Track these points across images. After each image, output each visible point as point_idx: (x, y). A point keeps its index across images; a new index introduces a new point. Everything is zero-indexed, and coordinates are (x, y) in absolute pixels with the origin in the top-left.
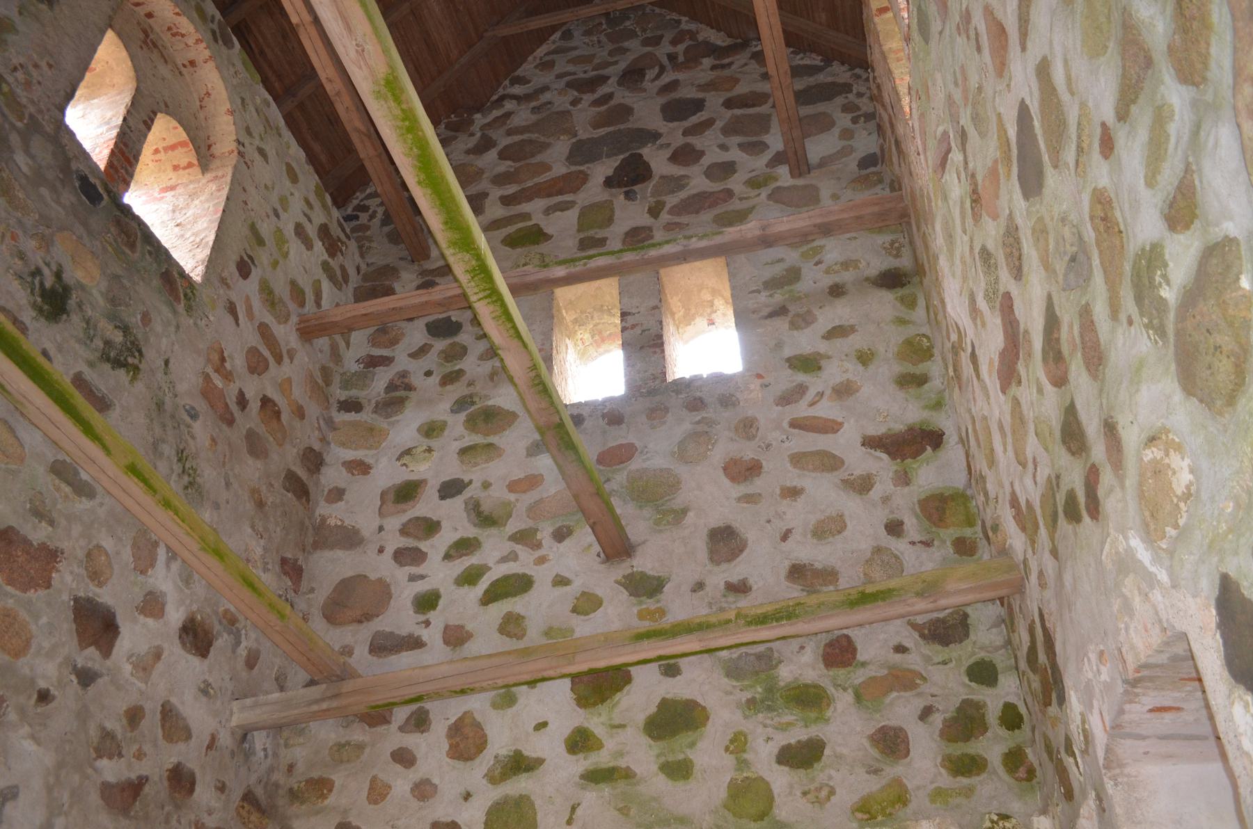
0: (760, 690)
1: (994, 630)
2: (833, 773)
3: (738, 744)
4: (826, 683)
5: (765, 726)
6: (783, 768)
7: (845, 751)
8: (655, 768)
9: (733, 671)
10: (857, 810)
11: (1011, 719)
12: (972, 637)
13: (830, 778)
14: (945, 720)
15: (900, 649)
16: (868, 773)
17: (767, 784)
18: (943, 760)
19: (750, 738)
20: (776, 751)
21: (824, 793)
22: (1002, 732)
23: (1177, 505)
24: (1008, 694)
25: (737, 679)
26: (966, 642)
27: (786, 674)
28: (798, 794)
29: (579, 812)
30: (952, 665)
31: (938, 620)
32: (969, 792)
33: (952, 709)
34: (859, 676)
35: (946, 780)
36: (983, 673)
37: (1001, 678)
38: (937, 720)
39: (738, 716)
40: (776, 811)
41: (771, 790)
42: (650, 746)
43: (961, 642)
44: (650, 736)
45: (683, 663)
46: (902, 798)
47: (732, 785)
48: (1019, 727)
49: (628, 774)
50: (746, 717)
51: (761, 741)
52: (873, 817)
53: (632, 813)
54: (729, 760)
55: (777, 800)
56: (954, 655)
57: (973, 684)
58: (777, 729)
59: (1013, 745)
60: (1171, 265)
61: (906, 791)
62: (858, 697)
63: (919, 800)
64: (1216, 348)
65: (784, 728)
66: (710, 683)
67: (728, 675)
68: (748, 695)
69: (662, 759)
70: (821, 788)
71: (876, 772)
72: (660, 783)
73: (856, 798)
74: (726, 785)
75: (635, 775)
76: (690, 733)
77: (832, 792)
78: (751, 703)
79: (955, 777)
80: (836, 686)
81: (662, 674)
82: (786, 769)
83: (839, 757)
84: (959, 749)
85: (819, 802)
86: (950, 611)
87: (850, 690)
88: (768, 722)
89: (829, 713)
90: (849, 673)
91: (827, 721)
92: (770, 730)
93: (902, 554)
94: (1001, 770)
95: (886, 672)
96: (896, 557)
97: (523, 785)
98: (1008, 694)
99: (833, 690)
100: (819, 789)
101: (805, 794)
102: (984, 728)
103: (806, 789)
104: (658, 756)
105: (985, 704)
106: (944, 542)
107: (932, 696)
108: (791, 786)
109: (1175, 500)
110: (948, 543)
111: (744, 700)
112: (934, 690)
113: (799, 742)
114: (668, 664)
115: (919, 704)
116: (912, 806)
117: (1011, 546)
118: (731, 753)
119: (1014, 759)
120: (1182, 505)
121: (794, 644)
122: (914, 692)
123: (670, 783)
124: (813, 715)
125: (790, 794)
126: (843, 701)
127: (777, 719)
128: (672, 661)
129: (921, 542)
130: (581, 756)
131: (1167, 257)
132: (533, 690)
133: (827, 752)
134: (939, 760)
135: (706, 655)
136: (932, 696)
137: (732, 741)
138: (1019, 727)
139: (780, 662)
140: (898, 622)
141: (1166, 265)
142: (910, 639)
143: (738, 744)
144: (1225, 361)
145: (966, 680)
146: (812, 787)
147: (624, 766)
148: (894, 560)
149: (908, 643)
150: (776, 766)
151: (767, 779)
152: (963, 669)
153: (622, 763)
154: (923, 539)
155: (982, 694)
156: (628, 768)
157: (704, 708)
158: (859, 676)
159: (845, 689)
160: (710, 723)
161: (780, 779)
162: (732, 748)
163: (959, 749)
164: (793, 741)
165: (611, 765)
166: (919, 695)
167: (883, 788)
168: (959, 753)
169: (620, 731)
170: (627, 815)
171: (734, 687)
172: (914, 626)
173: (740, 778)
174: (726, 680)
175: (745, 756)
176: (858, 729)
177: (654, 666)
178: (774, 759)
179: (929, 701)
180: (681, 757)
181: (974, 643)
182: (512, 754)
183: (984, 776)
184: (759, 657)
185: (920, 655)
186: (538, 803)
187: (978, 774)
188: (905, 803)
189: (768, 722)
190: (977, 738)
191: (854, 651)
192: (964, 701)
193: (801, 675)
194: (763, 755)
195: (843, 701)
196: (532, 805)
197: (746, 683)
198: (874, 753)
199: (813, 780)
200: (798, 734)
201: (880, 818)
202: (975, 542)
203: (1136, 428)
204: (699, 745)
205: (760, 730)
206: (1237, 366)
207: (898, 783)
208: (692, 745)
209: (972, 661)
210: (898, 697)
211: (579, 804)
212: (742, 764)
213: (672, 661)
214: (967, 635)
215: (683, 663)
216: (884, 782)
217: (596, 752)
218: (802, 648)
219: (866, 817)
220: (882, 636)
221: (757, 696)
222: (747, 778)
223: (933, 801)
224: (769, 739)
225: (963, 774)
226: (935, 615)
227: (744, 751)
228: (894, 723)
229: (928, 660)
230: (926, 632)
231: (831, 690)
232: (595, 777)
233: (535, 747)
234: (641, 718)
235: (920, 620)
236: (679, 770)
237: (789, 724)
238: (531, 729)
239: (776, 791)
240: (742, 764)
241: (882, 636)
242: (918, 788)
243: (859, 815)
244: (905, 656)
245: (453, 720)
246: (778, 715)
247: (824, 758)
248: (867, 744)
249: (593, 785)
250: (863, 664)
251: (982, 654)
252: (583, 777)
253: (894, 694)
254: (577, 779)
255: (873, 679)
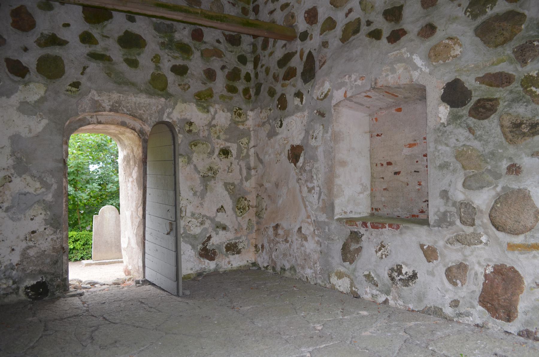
0: (167, 40)
1: (248, 46)
2: (190, 80)
3: (156, 59)
4: (191, 45)
5: (168, 55)
6: (172, 73)
7: (195, 73)
8: (122, 59)
9: (157, 28)
10: (197, 95)
11: (248, 78)
12: (241, 46)
13: (189, 82)
14: (228, 72)
15: (218, 41)
16: (202, 83)
17: (166, 78)
18: (226, 86)
19: (161, 58)
20: (171, 66)
21: (186, 87)
22: (244, 81)
23: (449, 57)
24: (248, 69)
25: (159, 33)
26: (239, 47)
27: (177, 36)
28: (177, 85)
29: (88, 70)
30: (234, 53)
31: (232, 35)
32: (231, 98)
33: (231, 69)
34: (203, 47)
35: (225, 92)
36: (242, 60)
37: (248, 63)
38: (226, 71)
39: (158, 48)
40: (168, 89)
41: (167, 81)
42: (120, 50)
43: (237, 46)
44: (120, 45)
45: (137, 17)
46: (211, 95)
47: (153, 75)
48: (250, 82)
49: (109, 59)
50: (161, 49)
51: (166, 61)
52: (201, 99)
53: (112, 76)
54: (153, 65)
55: (169, 85)
56: (235, 50)
57: (239, 62)
58: (172, 57)
59: (247, 87)
60: (496, 6)
61: (213, 93)
62: (202, 55)
63: (216, 97)
64: (502, 34)
65: (175, 58)
66: (148, 30)
67: (155, 29)
68: (162, 40)
69: (125, 57)
70: (186, 85)
71: (205, 84)
72: (124, 67)
73: (196, 91)
74: (150, 74)
75: (112, 60)
76: (138, 49)
77: (189, 87)
78: (163, 44)
79: (228, 92)
80: (195, 48)
81: (127, 19)
82: (174, 74)
83: (193, 75)
84: (231, 83)
85: (184, 90)
86: (236, 33)
87: (200, 51)
88: (169, 54)
89: (191, 57)
90: (200, 44)
91: (190, 60)
92: (170, 57)
93: (225, 5)
94: (242, 94)
95: (213, 48)
96: (222, 5)
97: (58, 51)
98: (248, 69)
99: (194, 49)
100: (185, 85)
101: (179, 85)
102: (239, 79)
103: (180, 83)
104: (123, 55)
105: (241, 71)
106: (239, 7)
107: (226, 62)
108: (175, 81)
109: (449, 56)
110: (240, 7)
111: (160, 42)
112: (227, 60)
113: (180, 65)
114: (130, 16)
115: (221, 64)
116: (214, 99)
117: (296, 25)
118: (154, 62)
119: (246, 91)
120: (451, 58)
121: (182, 25)
122: (221, 59)
123: (129, 68)
124: (186, 56)
125: (174, 84)
126: (197, 54)
127: (173, 54)
128: (132, 15)
129: (232, 3)
130: (87, 45)
131: (497, 3)
132: (63, 6)
133: (189, 72)
134: (225, 85)
135: (147, 18)
136: (226, 62)
137: (154, 57)
138: (250, 82)
139: (176, 31)
140: (219, 31)
141: (495, 5)
142: (222, 39)
143: (156, 59)
144: (502, 38)
145: (237, 60)
146: (183, 83)
147: (108, 55)
148: (221, 6)
149: (221, 40)
150: (170, 72)
151: (167, 76)
152: (237, 56)
153: (108, 54)
154: (233, 2)
155: (241, 67)
156: (110, 56)
157: (144, 40)
158: (203, 47)
159: (198, 50)
160: (146, 48)
161: (171, 77)
162: (154, 60)
163: (231, 83)
164: (178, 64)
165: (102, 53)
166: (222, 60)
167: (205, 90)
168: (231, 84)
169: (107, 39)
170: (110, 77)
171: (157, 35)
172: (224, 35)
173: (157, 73)
174: (154, 31)
175: (159, 65)
176: (201, 66)
177: (124, 14)
178: (170, 69)
179: (225, 64)
180: (134, 58)
181: (242, 48)
182: (51, 34)
183: (236, 94)
184: (168, 26)
185: (224, 46)
186: (66, 61)
187: (235, 93)
188: (212, 97)
189: (169, 54)
190: (236, 81)
191: (203, 36)
192: (235, 68)
193: (183, 39)
194: (166, 65)
195: (197, 54)
196: (62, 62)
197: (161, 35)
198: (204, 76)
199: (183, 81)
200: (179, 62)
201: (203, 100)
202: (248, 11)
203: (444, 33)
204: (142, 55)
205: (166, 56)
206: (505, 41)
207: (210, 89)
208: (139, 54)
209: (240, 54)
210: (216, 59)
211: (88, 67)
212: (158, 68)
213: (132, 15)
214: (240, 44)
215: (137, 17)
216: (207, 88)
217: (95, 45)
218: (185, 28)
219: (199, 98)
220: (213, 34)
221: (166, 42)
222: (159, 74)
223: (220, 98)
224: (169, 61)
225: (231, 92)
226: (232, 33)
227: (159, 63)
228: (213, 68)
229: (226, 48)
230: (228, 38)
231: (193, 49)
232: (95, 56)
233: (63, 34)
234: (116, 36)
235: (227, 33)
236: (133, 63)
237: (177, 57)
238: (61, 25)
239: (169, 82)
240: (158, 68)
241: (213, 34)
242: (216, 93)
243: (197, 97)
244: (220, 44)
245: (15, 7)
246: (174, 52)
247: (187, 74)
248: (202, 73)
249: (94, 60)
250: (205, 43)
251: (244, 53)
252: (88, 55)
253: (214, 58)
254: (86, 55)
255: (207, 49)
